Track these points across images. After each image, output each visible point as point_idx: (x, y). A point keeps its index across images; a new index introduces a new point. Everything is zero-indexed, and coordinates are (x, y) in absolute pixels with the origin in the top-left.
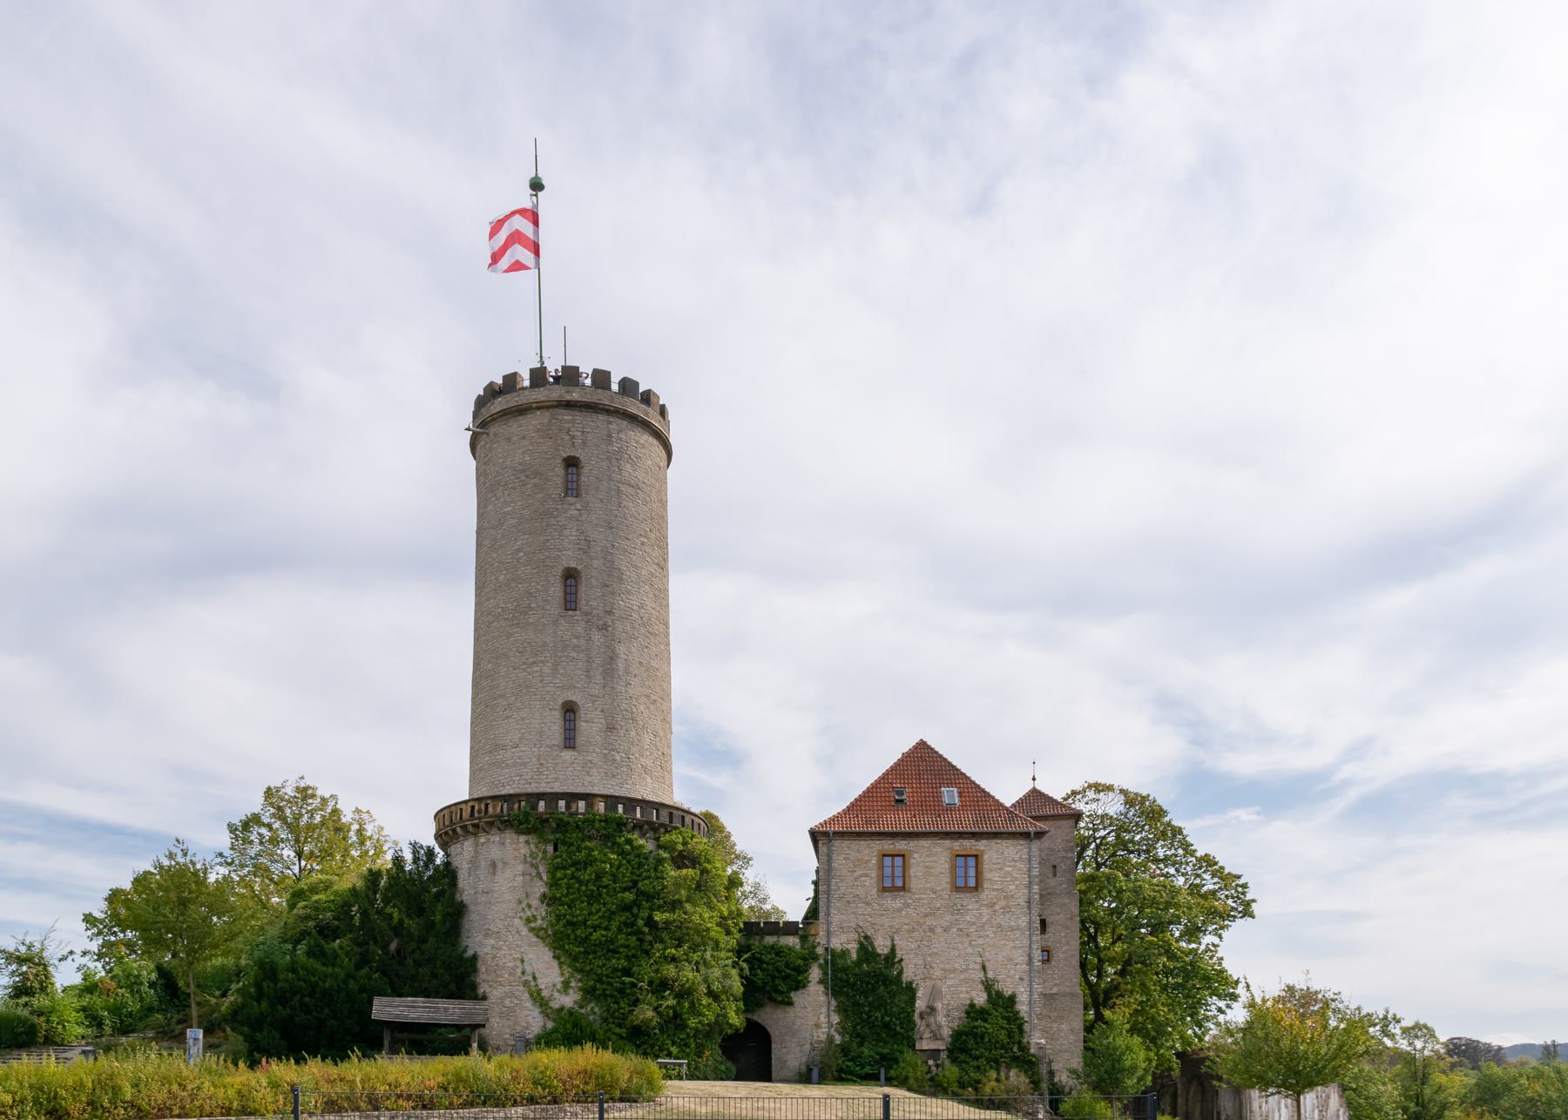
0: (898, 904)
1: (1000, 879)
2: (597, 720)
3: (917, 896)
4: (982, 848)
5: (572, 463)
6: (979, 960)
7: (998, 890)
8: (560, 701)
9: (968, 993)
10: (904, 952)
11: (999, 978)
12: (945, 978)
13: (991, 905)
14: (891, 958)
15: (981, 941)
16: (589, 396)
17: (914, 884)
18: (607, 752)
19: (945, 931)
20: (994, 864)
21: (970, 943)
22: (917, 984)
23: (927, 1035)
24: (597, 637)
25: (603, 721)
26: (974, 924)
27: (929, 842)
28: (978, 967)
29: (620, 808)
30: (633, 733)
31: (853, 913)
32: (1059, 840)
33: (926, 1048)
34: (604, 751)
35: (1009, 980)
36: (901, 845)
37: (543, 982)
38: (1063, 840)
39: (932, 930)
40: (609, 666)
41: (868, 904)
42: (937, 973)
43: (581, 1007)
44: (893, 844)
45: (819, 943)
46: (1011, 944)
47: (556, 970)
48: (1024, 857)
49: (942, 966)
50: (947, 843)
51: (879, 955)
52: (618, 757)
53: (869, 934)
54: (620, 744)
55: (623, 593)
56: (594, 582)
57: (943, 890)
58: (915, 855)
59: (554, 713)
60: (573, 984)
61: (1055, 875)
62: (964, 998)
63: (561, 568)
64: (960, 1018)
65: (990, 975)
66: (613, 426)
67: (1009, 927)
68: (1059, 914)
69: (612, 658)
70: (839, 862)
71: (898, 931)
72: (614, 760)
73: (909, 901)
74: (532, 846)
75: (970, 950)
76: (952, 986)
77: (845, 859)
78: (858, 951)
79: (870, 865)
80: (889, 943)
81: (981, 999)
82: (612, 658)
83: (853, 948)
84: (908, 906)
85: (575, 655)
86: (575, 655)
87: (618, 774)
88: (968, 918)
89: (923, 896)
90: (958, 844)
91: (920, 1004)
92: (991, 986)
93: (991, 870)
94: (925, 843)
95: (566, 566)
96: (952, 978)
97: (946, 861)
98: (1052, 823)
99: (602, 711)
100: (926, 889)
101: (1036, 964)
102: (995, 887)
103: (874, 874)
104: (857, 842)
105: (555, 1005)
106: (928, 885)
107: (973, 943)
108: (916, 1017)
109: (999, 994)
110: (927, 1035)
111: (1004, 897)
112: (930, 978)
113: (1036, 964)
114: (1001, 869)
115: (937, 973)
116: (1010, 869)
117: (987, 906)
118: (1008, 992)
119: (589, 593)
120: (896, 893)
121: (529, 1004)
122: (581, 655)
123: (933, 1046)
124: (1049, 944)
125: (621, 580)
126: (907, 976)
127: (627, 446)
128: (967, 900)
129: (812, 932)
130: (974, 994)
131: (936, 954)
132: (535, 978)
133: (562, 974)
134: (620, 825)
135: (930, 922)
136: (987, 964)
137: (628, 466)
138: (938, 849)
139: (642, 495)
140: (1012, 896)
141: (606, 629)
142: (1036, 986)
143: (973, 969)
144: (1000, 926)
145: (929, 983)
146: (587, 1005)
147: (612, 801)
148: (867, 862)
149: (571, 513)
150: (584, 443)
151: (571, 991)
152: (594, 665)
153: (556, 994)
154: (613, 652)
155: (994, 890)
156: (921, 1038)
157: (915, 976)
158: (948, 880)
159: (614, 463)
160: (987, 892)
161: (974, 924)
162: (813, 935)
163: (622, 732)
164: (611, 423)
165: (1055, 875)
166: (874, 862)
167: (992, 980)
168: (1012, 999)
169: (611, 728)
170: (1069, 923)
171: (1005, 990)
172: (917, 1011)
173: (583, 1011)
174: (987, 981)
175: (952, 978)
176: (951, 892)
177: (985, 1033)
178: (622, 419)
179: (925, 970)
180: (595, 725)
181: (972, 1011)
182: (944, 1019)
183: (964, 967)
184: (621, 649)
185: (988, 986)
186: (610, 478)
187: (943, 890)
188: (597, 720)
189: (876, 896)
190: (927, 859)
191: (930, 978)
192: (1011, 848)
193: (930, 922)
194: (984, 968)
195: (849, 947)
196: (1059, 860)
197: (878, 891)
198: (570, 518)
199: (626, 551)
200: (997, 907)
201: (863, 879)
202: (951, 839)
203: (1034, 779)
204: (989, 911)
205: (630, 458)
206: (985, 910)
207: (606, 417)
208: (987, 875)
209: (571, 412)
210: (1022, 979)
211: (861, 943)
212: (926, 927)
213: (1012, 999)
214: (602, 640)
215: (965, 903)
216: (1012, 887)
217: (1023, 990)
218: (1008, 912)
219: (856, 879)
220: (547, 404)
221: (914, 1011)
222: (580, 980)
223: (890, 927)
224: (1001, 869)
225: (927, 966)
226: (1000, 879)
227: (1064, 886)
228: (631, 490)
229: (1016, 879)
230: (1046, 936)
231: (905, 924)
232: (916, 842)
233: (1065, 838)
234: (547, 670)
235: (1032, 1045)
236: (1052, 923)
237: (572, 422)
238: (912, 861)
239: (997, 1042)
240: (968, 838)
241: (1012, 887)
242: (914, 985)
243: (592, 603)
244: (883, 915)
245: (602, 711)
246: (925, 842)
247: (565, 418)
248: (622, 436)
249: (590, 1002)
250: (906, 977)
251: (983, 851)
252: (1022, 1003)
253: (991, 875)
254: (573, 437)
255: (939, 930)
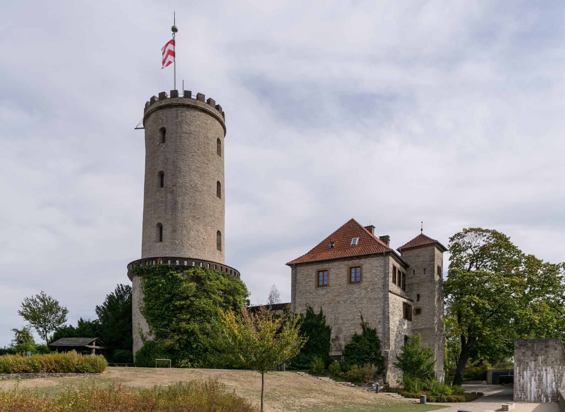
0: (324, 292)
1: (371, 276)
2: (169, 229)
3: (332, 288)
4: (362, 263)
5: (163, 131)
6: (360, 314)
7: (369, 281)
8: (156, 224)
9: (354, 329)
10: (326, 313)
11: (369, 322)
12: (344, 323)
13: (366, 289)
14: (321, 316)
15: (361, 306)
16: (168, 102)
17: (331, 283)
18: (172, 240)
19: (344, 302)
20: (367, 269)
21: (356, 307)
22: (332, 327)
23: (334, 349)
24: (169, 196)
25: (171, 229)
26: (357, 298)
27: (338, 263)
28: (359, 317)
29: (177, 262)
30: (185, 232)
31: (305, 298)
32: (427, 257)
33: (334, 355)
34: (171, 241)
35: (374, 322)
36: (326, 266)
37: (144, 332)
38: (429, 256)
39: (338, 302)
40: (174, 207)
41: (311, 293)
42: (340, 322)
43: (156, 341)
44: (322, 266)
45: (291, 312)
46: (375, 306)
47: (148, 327)
48: (382, 264)
49: (343, 318)
50: (346, 262)
51: (315, 315)
52: (177, 242)
53: (311, 306)
54: (178, 237)
55: (182, 177)
56: (169, 175)
57: (344, 284)
58: (332, 270)
59: (154, 228)
60: (153, 332)
61: (425, 273)
62: (352, 332)
63: (157, 172)
64: (350, 341)
65: (365, 321)
66: (179, 111)
67: (374, 298)
68: (426, 291)
69: (175, 203)
70: (299, 276)
71: (323, 304)
72: (176, 243)
73: (329, 290)
74: (141, 280)
75: (355, 310)
76: (347, 327)
77: (302, 275)
78: (307, 314)
79: (312, 276)
80: (320, 310)
81: (360, 332)
82: (176, 203)
83: (305, 312)
84: (328, 292)
85: (161, 204)
86: (161, 204)
87: (177, 249)
88: (355, 296)
89: (335, 288)
90: (351, 262)
91: (333, 336)
92: (365, 326)
93: (366, 273)
94: (336, 264)
95: (159, 171)
96: (347, 324)
97: (345, 271)
98: (424, 249)
99: (171, 225)
100: (336, 284)
101: (386, 314)
102: (368, 280)
103: (314, 280)
104: (307, 267)
105: (147, 340)
106: (337, 282)
107: (357, 307)
108: (331, 342)
109: (369, 330)
110: (334, 349)
111: (372, 284)
112: (337, 324)
113: (386, 314)
114: (370, 272)
115: (340, 322)
116: (375, 271)
117: (364, 289)
118: (373, 328)
119: (167, 180)
120: (323, 287)
121: (140, 340)
122: (163, 204)
123: (336, 354)
124: (421, 306)
125: (181, 171)
126: (328, 323)
127: (185, 118)
128: (355, 287)
129: (288, 307)
130: (357, 330)
131: (340, 313)
132: (142, 330)
133: (149, 328)
134: (168, 268)
135: (338, 299)
136: (363, 316)
137: (186, 126)
138: (342, 266)
139: (192, 136)
140: (376, 284)
141: (173, 192)
142: (386, 325)
143: (357, 319)
144: (370, 298)
145: (337, 326)
146: (158, 339)
147: (165, 259)
148: (312, 275)
149: (161, 149)
150: (167, 121)
151: (152, 335)
152: (168, 207)
153: (148, 336)
154: (176, 201)
155: (367, 281)
156: (332, 351)
157: (331, 323)
158: (346, 279)
159: (179, 125)
160: (364, 283)
161: (357, 298)
162: (288, 309)
163: (179, 232)
164: (178, 110)
165: (425, 273)
166: (314, 275)
167: (365, 323)
168: (374, 332)
169: (174, 231)
170: (430, 295)
171: (372, 327)
172: (331, 339)
173: (157, 342)
174: (363, 324)
175: (347, 324)
176: (348, 284)
177: (356, 347)
178: (183, 108)
179: (335, 321)
180: (168, 231)
181: (356, 338)
182: (343, 342)
183: (353, 318)
184: (180, 200)
185: (363, 326)
186: (177, 132)
187: (344, 284)
188: (169, 229)
189: (314, 289)
190: (337, 271)
191: (337, 324)
192: (376, 261)
193: (338, 299)
194: (362, 318)
195: (303, 312)
196: (427, 266)
197: (316, 287)
198: (161, 152)
199: (183, 160)
200: (369, 289)
201: (309, 282)
202: (348, 260)
203: (422, 230)
204: (365, 292)
205: (187, 122)
206: (363, 291)
207: (176, 109)
208: (364, 275)
209: (162, 110)
210: (380, 322)
211: (308, 310)
212: (336, 302)
213: (374, 332)
214: (171, 197)
215: (354, 289)
216: (376, 279)
217: (380, 327)
218: (374, 291)
219: (307, 283)
220: (154, 109)
221: (330, 339)
222: (155, 330)
223: (321, 303)
224: (370, 272)
225: (336, 319)
226: (371, 276)
227: (429, 278)
228: (186, 135)
229: (378, 275)
230: (419, 302)
231: (327, 301)
232: (332, 264)
233: (431, 255)
234: (152, 213)
235: (383, 352)
236: (422, 296)
237: (162, 114)
238: (331, 272)
239: (363, 351)
240: (356, 259)
241: (376, 279)
242: (330, 328)
243: (167, 183)
244: (317, 298)
245: (171, 225)
246: (336, 263)
247: (160, 113)
248: (183, 114)
249: (159, 338)
250: (326, 324)
251: (362, 265)
252: (380, 333)
253: (367, 275)
254: (163, 120)
255: (342, 302)
